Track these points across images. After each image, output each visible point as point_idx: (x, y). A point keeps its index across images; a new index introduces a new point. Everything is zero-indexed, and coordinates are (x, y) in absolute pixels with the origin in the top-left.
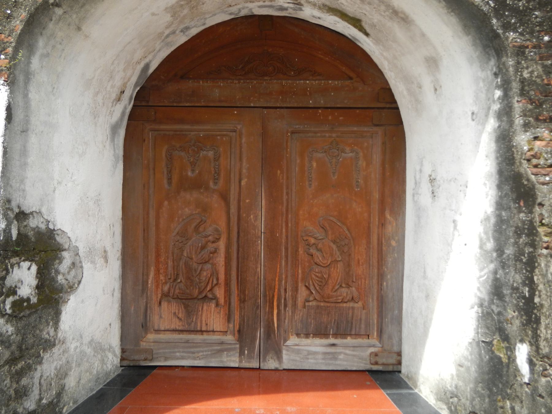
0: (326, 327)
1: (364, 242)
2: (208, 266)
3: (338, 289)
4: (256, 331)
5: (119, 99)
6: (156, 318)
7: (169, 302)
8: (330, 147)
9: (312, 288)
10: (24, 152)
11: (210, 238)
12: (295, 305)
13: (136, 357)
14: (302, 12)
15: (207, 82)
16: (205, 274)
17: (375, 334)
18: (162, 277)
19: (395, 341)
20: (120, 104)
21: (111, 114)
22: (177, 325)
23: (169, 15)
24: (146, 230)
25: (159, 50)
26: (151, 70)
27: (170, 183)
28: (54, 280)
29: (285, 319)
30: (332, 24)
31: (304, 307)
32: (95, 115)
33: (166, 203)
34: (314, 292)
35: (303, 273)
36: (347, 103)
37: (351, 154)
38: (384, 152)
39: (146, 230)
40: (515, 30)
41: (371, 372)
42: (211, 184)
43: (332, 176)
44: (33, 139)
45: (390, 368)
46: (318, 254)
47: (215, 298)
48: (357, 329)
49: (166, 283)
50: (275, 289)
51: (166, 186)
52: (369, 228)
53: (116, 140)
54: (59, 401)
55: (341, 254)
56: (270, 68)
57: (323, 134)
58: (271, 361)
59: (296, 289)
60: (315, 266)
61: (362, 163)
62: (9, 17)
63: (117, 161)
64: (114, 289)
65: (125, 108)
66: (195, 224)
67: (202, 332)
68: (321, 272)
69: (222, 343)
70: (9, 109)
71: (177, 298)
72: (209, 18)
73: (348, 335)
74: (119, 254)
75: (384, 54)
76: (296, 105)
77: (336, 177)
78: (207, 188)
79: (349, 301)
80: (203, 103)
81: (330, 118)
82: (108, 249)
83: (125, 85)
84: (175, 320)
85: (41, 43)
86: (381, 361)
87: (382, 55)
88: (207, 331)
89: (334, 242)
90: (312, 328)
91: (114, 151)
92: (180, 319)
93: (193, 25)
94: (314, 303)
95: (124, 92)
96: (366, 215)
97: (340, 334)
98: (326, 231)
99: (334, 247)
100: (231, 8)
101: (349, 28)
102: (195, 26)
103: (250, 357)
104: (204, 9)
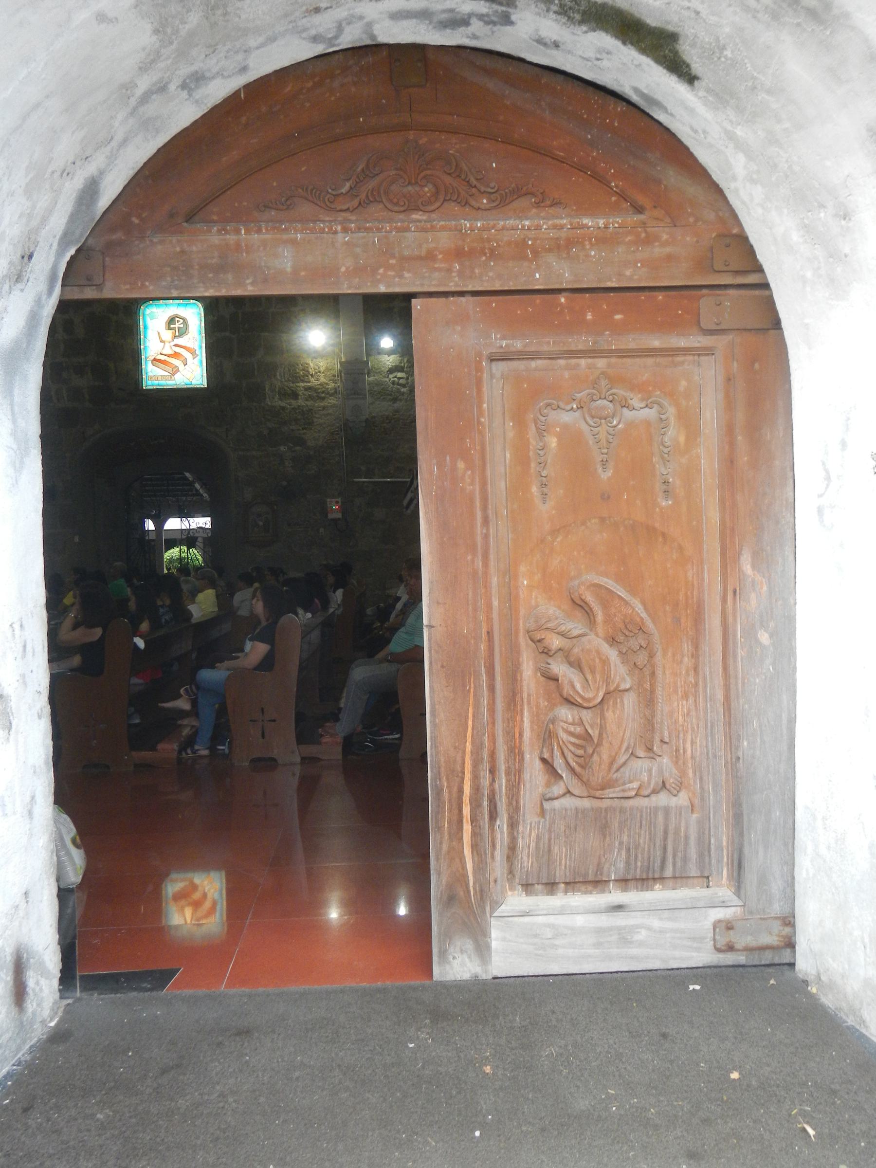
3: (624, 763)
8: (593, 394)
14: (508, 28)
15: (259, 231)
17: (725, 872)
19: (776, 886)
20: (22, 290)
23: (148, 27)
25: (124, 142)
26: (104, 202)
29: (494, 846)
30: (587, 60)
31: (543, 813)
34: (564, 775)
37: (647, 410)
43: (600, 470)
45: (768, 957)
48: (679, 864)
50: (464, 773)
53: (16, 392)
55: (631, 673)
56: (426, 189)
57: (573, 361)
61: (674, 434)
64: (33, 798)
65: (38, 303)
72: (257, 48)
73: (654, 879)
75: (739, 132)
76: (497, 286)
77: (609, 473)
79: (655, 792)
80: (250, 288)
81: (589, 317)
86: (742, 940)
87: (731, 136)
89: (612, 641)
91: (14, 422)
93: (214, 71)
95: (31, 257)
97: (636, 879)
99: (613, 654)
100: (317, 19)
101: (639, 66)
102: (220, 74)
104: (243, 17)
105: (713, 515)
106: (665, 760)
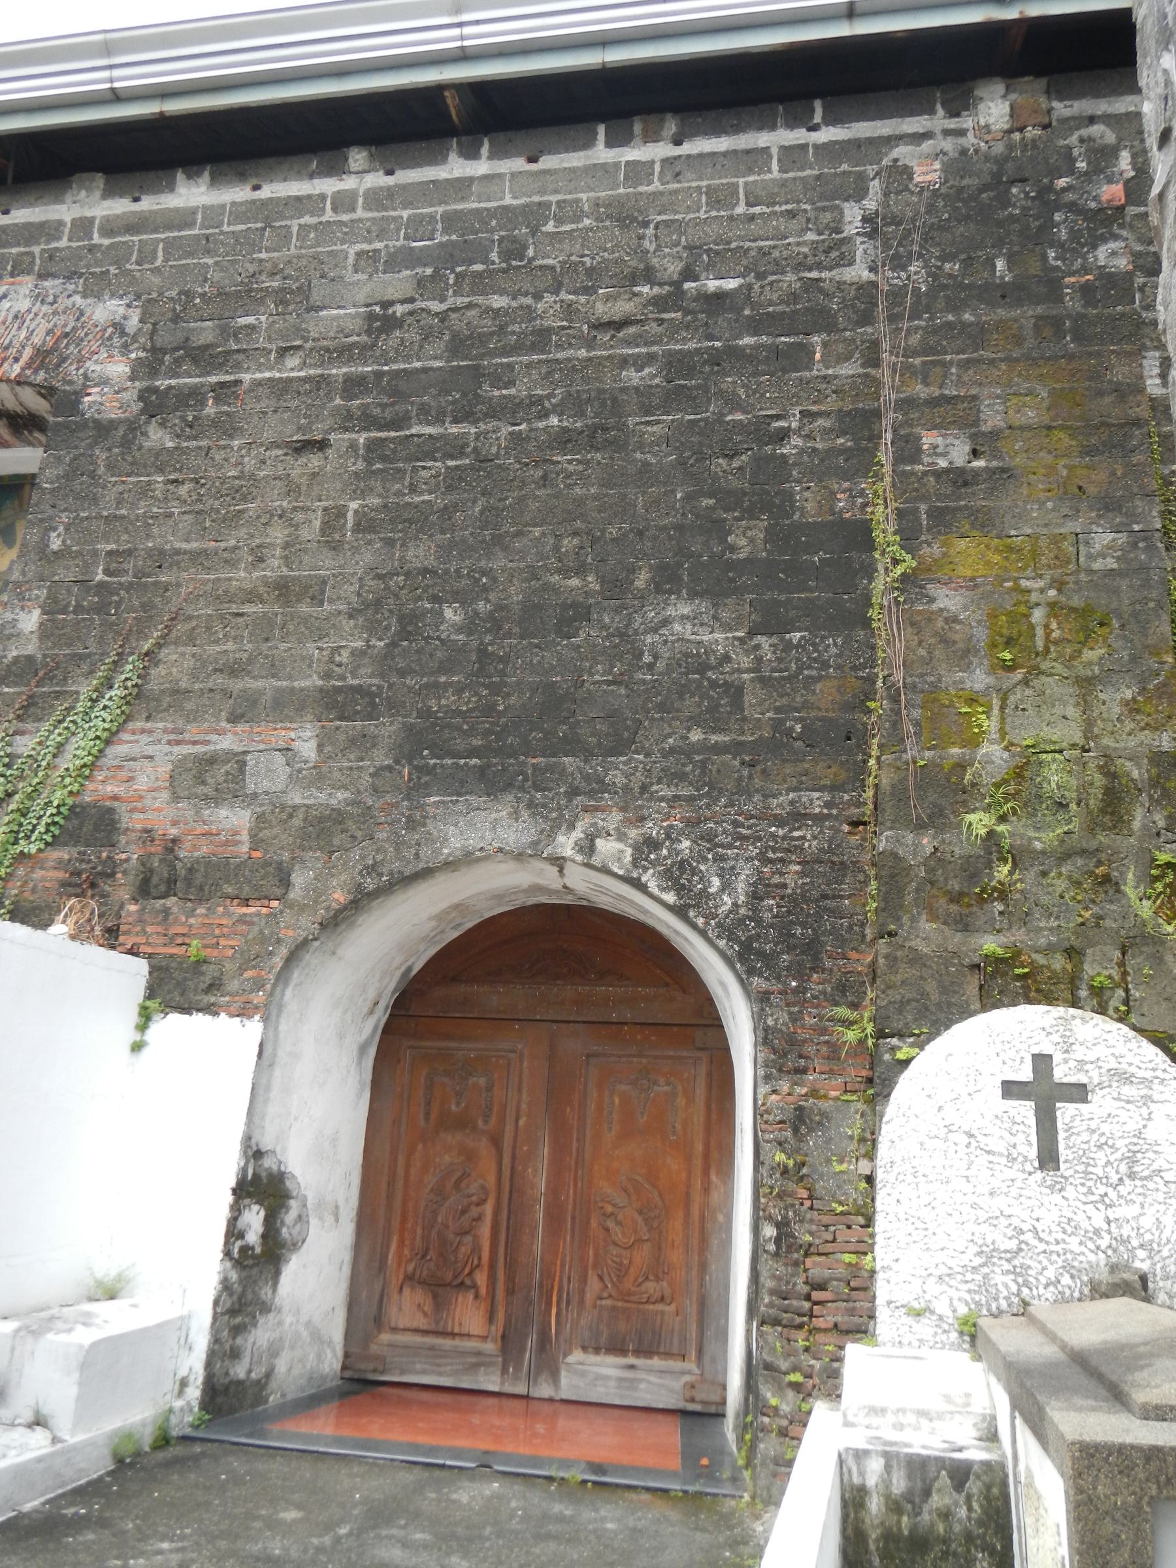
0: (624, 1340)
1: (681, 1214)
2: (468, 1239)
4: (527, 1336)
5: (371, 1012)
6: (393, 1312)
7: (413, 1288)
9: (606, 1278)
10: (268, 1089)
11: (474, 1198)
12: (582, 1302)
13: (363, 1366)
16: (463, 1249)
18: (406, 1252)
21: (360, 1031)
22: (421, 1322)
24: (391, 1183)
27: (427, 1119)
28: (278, 1232)
31: (595, 1306)
32: (341, 1036)
33: (420, 1146)
35: (596, 1255)
36: (661, 1018)
37: (666, 1088)
38: (709, 1087)
39: (391, 1183)
40: (760, 975)
41: (684, 1413)
42: (480, 1123)
44: (277, 1072)
45: (713, 1409)
46: (618, 1229)
47: (474, 1286)
49: (410, 1260)
51: (422, 1123)
52: (688, 1194)
54: (266, 1384)
58: (545, 1385)
59: (584, 1279)
60: (612, 1247)
61: (681, 1101)
62: (271, 953)
63: (362, 1090)
66: (453, 1180)
67: (453, 1335)
68: (618, 1256)
69: (479, 1353)
70: (261, 1046)
71: (423, 1283)
74: (353, 1214)
76: (594, 1019)
78: (475, 1128)
82: (341, 1204)
83: (380, 995)
84: (419, 1315)
85: (296, 974)
88: (461, 1335)
89: (640, 1213)
90: (603, 1340)
92: (425, 1314)
94: (609, 1302)
96: (684, 1174)
98: (629, 1196)
99: (640, 1219)
103: (516, 1378)
105: (699, 1147)
106: (665, 1284)
